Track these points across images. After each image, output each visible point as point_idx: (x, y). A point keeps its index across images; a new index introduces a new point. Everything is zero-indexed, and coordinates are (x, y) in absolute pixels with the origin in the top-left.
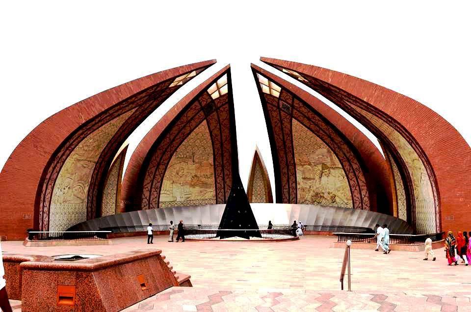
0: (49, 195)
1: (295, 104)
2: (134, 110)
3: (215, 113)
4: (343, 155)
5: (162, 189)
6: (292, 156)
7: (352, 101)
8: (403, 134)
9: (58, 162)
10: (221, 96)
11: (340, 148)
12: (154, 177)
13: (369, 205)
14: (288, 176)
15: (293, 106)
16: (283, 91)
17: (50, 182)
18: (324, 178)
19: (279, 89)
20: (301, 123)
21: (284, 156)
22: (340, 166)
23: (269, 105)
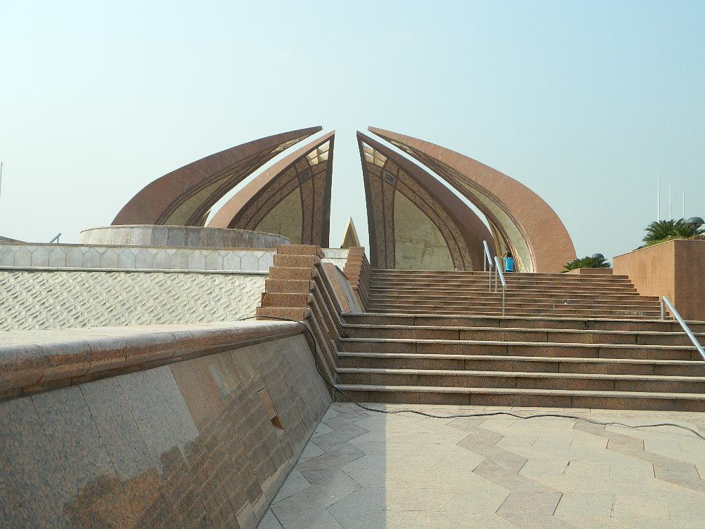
1: (400, 176)
6: (391, 231)
10: (320, 163)
15: (397, 177)
18: (427, 257)
21: (383, 231)
23: (370, 174)
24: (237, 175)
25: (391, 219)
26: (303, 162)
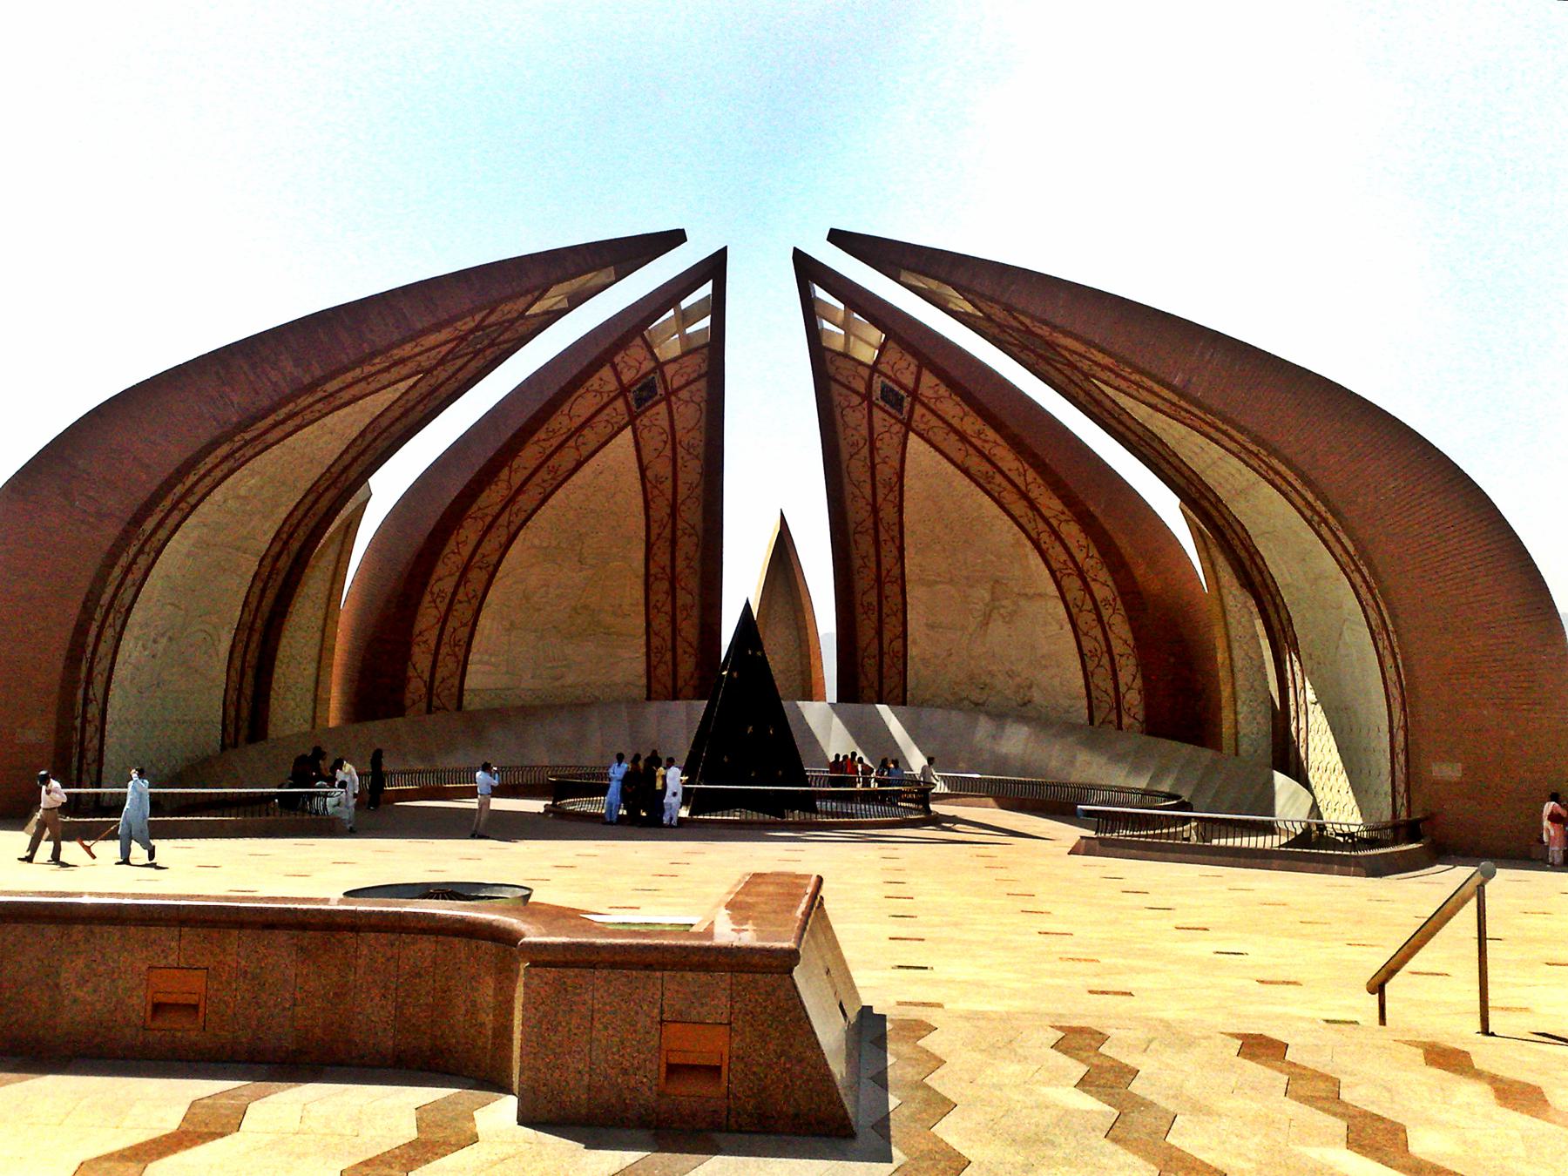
2: (403, 386)
4: (1064, 557)
5: (474, 650)
6: (895, 552)
7: (1124, 385)
9: (140, 551)
11: (1056, 534)
13: (1140, 716)
14: (880, 620)
15: (914, 394)
16: (891, 344)
17: (110, 619)
18: (998, 629)
19: (877, 336)
20: (937, 449)
21: (872, 551)
22: (1052, 589)
23: (835, 387)
24: (423, 388)
25: (894, 517)
26: (636, 351)
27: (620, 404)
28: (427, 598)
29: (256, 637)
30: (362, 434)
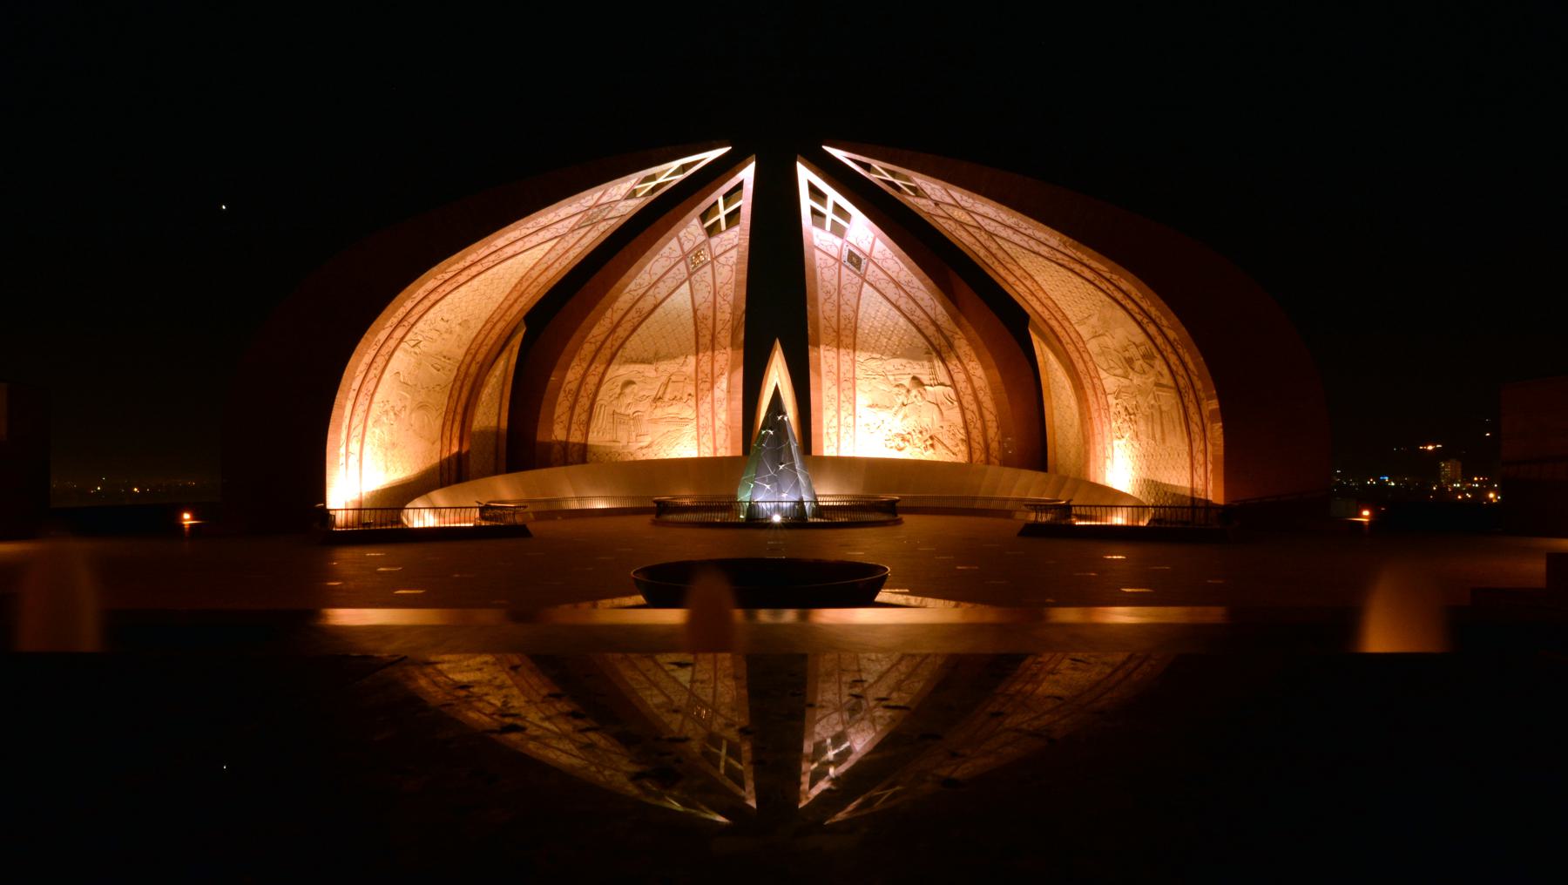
0: (360, 429)
2: (547, 246)
3: (708, 268)
4: (956, 362)
7: (1016, 238)
8: (1130, 306)
12: (576, 401)
15: (869, 257)
24: (560, 249)
25: (849, 341)
27: (682, 264)
28: (562, 394)
29: (458, 418)
30: (520, 282)
